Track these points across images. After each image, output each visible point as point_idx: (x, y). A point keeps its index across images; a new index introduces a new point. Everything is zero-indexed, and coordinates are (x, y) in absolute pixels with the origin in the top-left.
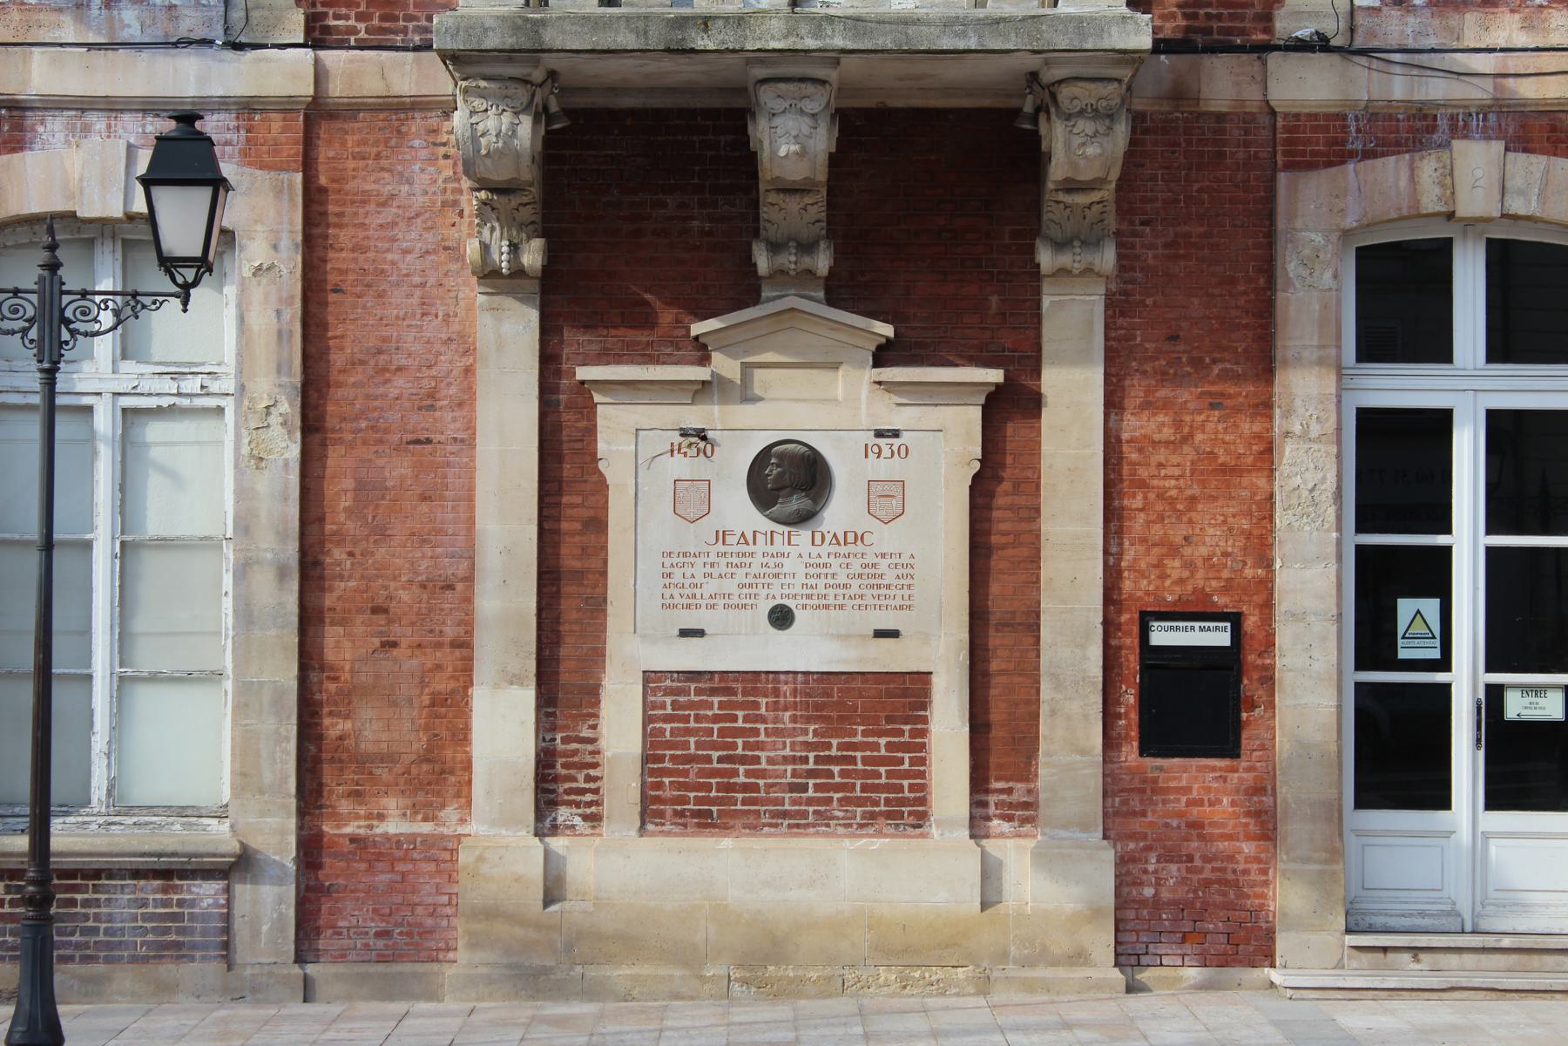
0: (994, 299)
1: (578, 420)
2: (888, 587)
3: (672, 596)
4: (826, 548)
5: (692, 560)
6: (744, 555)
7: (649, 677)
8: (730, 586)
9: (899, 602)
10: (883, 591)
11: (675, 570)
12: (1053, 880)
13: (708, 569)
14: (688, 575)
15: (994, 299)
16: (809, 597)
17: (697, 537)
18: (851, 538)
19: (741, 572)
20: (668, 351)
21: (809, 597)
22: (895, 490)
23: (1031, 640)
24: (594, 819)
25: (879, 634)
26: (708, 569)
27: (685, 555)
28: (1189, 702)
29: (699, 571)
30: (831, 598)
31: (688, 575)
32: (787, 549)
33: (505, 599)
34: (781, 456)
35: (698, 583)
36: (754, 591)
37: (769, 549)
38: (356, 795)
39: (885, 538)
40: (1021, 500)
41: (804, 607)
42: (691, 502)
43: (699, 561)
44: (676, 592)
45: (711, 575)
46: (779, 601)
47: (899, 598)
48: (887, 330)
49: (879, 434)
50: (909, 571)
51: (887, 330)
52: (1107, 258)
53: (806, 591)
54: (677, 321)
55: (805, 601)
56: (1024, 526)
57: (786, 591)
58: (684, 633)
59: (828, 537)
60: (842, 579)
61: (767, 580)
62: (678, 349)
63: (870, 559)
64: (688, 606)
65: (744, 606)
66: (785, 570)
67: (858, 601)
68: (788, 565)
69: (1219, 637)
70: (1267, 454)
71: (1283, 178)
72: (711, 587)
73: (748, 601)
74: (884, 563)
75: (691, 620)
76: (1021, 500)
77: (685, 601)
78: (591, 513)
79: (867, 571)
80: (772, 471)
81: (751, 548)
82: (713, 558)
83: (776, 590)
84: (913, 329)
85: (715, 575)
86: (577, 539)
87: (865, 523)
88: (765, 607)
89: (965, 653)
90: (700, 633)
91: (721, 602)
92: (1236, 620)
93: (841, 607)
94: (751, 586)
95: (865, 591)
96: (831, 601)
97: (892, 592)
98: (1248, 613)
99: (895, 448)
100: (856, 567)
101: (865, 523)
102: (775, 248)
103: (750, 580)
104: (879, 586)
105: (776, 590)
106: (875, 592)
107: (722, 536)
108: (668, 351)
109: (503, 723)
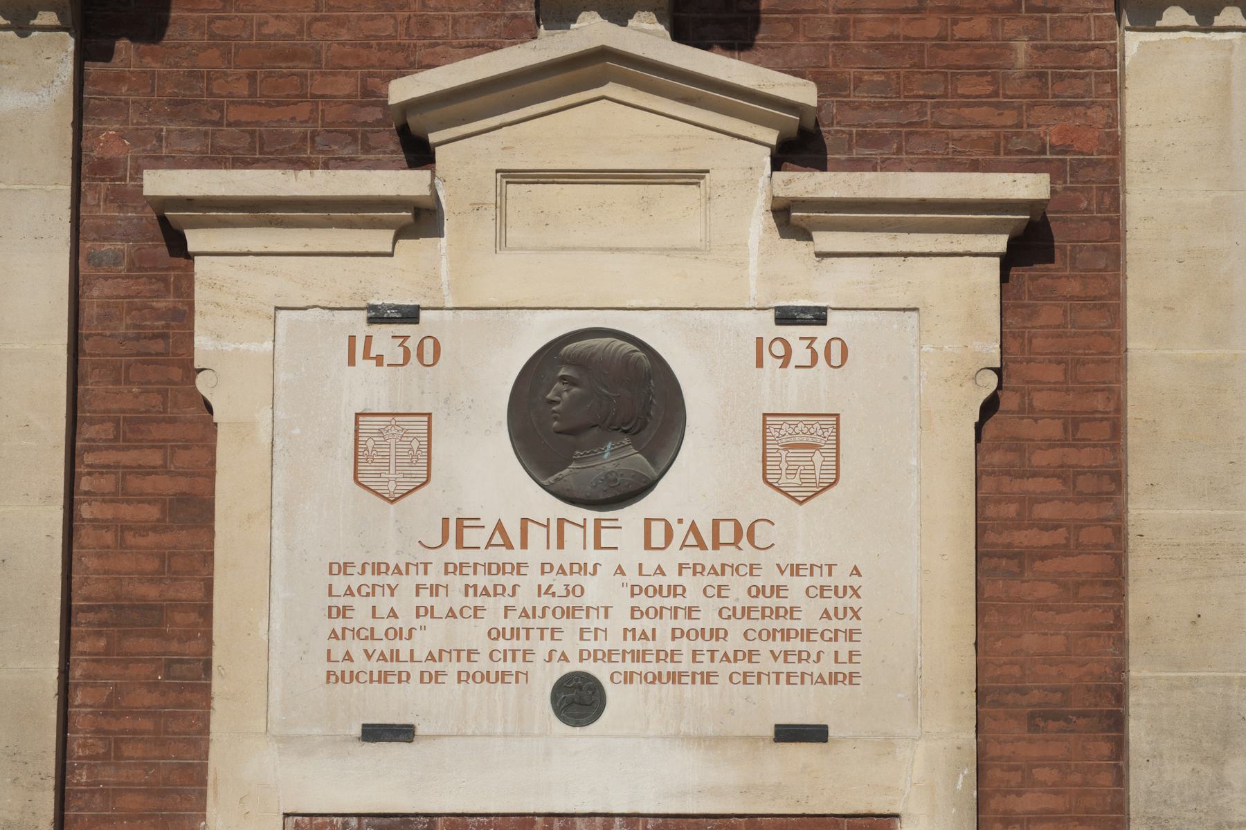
0: (1022, 48)
1: (157, 295)
2: (806, 635)
3: (348, 657)
4: (673, 556)
5: (391, 579)
6: (501, 569)
8: (471, 634)
9: (827, 666)
10: (796, 644)
11: (356, 601)
13: (426, 599)
14: (383, 610)
15: (1022, 48)
16: (639, 656)
17: (400, 531)
18: (727, 533)
20: (346, 153)
21: (639, 656)
22: (819, 432)
23: (1106, 748)
25: (787, 734)
26: (426, 599)
27: (377, 569)
29: (406, 602)
30: (686, 658)
31: (383, 610)
32: (592, 556)
34: (581, 362)
36: (521, 644)
39: (799, 533)
40: (1083, 458)
41: (629, 678)
43: (407, 583)
44: (356, 647)
45: (430, 612)
46: (574, 666)
47: (828, 659)
49: (786, 317)
53: (630, 645)
54: (366, 92)
55: (629, 666)
56: (1090, 510)
57: (591, 646)
58: (373, 733)
59: (680, 532)
60: (708, 619)
61: (550, 622)
62: (367, 149)
63: (770, 577)
64: (383, 677)
65: (502, 677)
66: (586, 601)
67: (743, 666)
68: (595, 590)
72: (431, 636)
73: (510, 666)
74: (796, 586)
75: (387, 707)
76: (1083, 458)
77: (376, 666)
78: (183, 484)
79: (761, 602)
80: (561, 394)
81: (516, 555)
83: (569, 642)
84: (855, 107)
85: (441, 610)
86: (152, 538)
88: (546, 677)
89: (970, 771)
90: (403, 733)
93: (707, 678)
94: (515, 633)
95: (757, 645)
96: (685, 664)
97: (813, 648)
99: (819, 347)
100: (738, 594)
101: (758, 502)
103: (514, 621)
104: (786, 635)
105: (569, 642)
106: (778, 646)
107: (455, 529)
108: (346, 153)
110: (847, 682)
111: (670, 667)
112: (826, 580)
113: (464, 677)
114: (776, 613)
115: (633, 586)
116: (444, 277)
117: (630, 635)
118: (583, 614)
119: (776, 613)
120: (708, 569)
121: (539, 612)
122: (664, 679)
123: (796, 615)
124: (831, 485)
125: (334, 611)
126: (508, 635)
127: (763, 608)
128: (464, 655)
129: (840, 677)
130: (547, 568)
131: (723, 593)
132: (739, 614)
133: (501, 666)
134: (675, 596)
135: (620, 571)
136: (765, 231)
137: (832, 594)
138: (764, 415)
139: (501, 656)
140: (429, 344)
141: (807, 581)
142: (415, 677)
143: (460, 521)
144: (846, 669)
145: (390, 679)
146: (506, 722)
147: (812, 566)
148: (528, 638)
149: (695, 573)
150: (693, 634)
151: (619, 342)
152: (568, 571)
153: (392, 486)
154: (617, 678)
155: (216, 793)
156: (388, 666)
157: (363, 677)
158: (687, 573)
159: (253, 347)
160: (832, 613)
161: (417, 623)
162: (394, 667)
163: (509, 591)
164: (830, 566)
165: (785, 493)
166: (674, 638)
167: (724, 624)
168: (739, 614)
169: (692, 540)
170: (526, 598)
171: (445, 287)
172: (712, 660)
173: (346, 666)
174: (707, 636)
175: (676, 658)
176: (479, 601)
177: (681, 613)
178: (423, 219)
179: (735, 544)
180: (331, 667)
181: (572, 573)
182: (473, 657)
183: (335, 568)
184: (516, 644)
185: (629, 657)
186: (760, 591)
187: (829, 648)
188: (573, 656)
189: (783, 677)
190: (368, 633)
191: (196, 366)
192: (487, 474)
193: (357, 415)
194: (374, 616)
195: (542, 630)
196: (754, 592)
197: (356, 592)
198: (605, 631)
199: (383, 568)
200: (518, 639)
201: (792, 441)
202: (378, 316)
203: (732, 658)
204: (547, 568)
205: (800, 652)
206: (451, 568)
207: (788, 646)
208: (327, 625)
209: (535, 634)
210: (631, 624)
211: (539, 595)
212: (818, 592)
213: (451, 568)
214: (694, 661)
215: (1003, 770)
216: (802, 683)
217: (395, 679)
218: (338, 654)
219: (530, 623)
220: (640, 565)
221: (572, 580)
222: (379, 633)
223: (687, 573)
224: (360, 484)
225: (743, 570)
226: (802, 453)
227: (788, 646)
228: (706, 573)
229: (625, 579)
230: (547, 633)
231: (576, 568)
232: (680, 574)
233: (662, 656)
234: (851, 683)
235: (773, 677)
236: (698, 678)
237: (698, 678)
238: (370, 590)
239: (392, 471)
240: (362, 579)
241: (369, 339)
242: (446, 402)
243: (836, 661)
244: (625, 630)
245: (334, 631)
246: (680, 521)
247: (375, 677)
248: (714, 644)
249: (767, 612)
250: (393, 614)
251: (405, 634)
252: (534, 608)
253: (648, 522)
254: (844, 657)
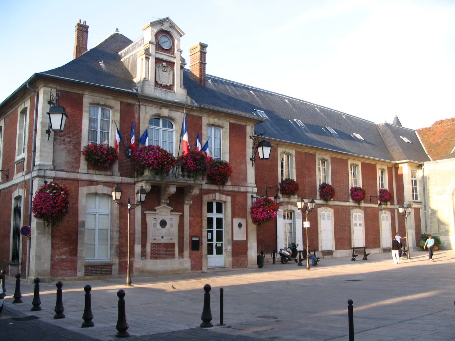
7: (151, 244)
12: (186, 263)
24: (146, 258)
28: (196, 246)
33: (138, 235)
35: (156, 234)
38: (124, 256)
39: (171, 229)
42: (155, 225)
48: (172, 209)
51: (172, 209)
52: (191, 202)
68: (163, 232)
69: (198, 239)
70: (202, 221)
71: (203, 196)
75: (155, 238)
92: (199, 237)
98: (200, 236)
101: (170, 228)
102: (164, 200)
109: (138, 248)
178: (156, 214)
192: (159, 226)
226: (171, 225)
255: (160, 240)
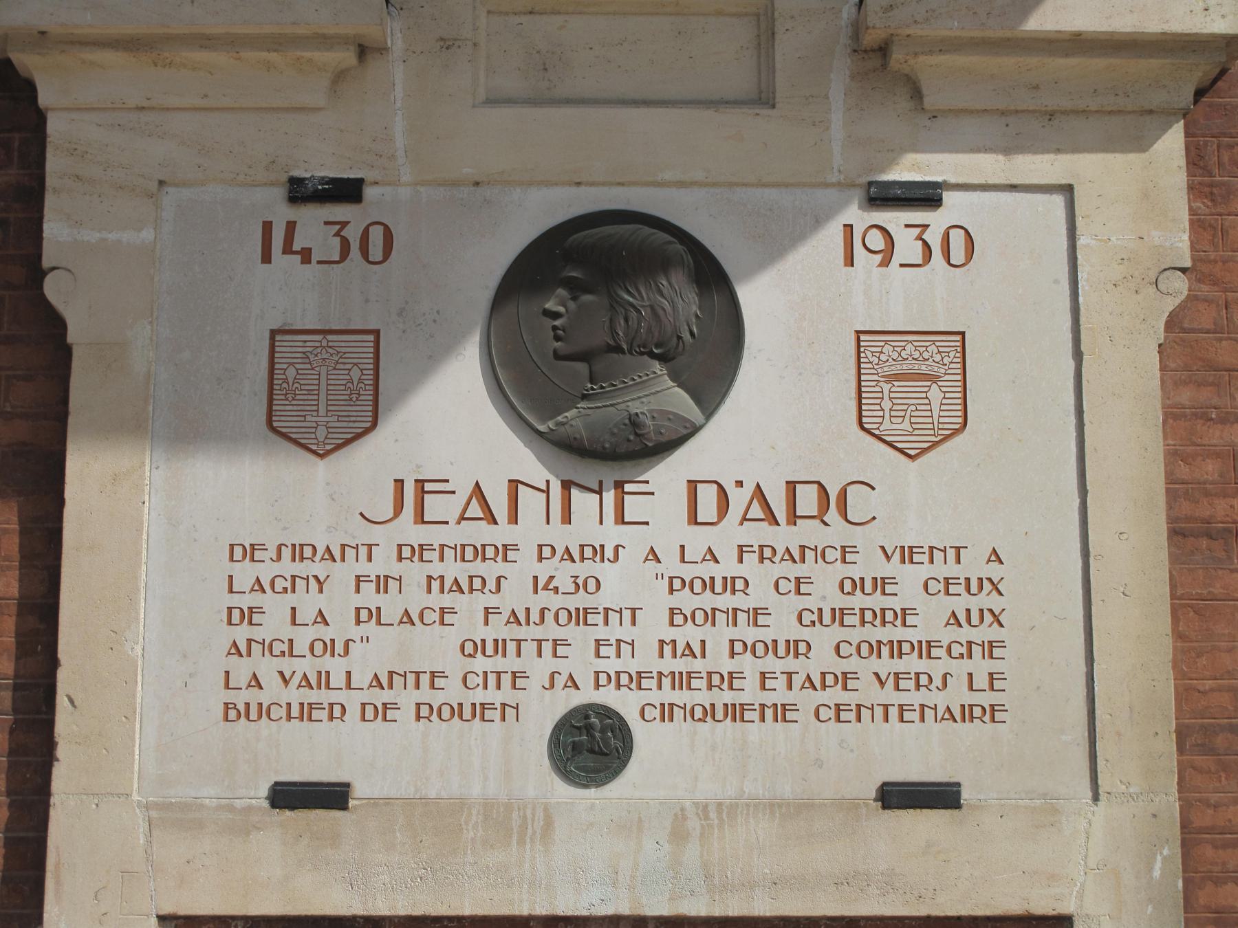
2: (925, 649)
3: (255, 682)
4: (728, 535)
6: (480, 553)
8: (436, 648)
9: (958, 695)
10: (912, 663)
11: (267, 600)
13: (369, 597)
14: (307, 614)
16: (682, 681)
18: (807, 500)
19: (469, 606)
21: (682, 681)
22: (936, 356)
26: (369, 597)
27: (298, 553)
29: (340, 600)
30: (750, 683)
32: (611, 534)
36: (509, 663)
37: (559, 535)
39: (911, 501)
41: (667, 712)
44: (267, 668)
45: (376, 615)
46: (587, 695)
47: (958, 686)
50: (987, 600)
53: (670, 664)
55: (669, 695)
57: (612, 665)
59: (739, 499)
60: (782, 626)
61: (551, 630)
63: (868, 566)
64: (307, 712)
66: (603, 599)
67: (835, 695)
68: (617, 584)
72: (376, 652)
73: (493, 696)
74: (909, 579)
75: (309, 756)
77: (295, 695)
79: (858, 601)
81: (501, 533)
82: (384, 563)
83: (578, 660)
85: (392, 613)
87: (850, 457)
88: (544, 711)
91: (407, 698)
93: (782, 712)
94: (500, 647)
96: (749, 693)
97: (937, 669)
101: (850, 457)
103: (498, 629)
104: (896, 649)
105: (579, 660)
106: (886, 665)
107: (414, 495)
110: (987, 718)
111: (728, 697)
112: (952, 570)
113: (425, 711)
114: (881, 617)
115: (671, 578)
116: (400, 142)
117: (668, 649)
118: (600, 619)
119: (881, 617)
120: (780, 551)
121: (535, 617)
122: (720, 715)
123: (910, 620)
124: (956, 432)
125: (236, 614)
126: (490, 650)
127: (862, 610)
128: (425, 679)
129: (977, 712)
130: (547, 552)
131: (803, 588)
132: (827, 619)
133: (479, 696)
134: (734, 591)
135: (653, 555)
136: (852, 78)
137: (961, 589)
138: (858, 332)
139: (480, 680)
140: (376, 235)
141: (925, 571)
142: (354, 711)
143: (420, 483)
144: (986, 699)
145: (316, 714)
146: (486, 779)
147: (931, 548)
148: (519, 655)
149: (762, 559)
150: (760, 648)
151: (647, 230)
152: (577, 557)
153: (321, 433)
154: (651, 713)
155: (58, 882)
156: (313, 696)
157: (276, 712)
158: (751, 559)
159: (127, 236)
160: (962, 618)
161: (355, 632)
162: (323, 697)
163: (491, 585)
164: (958, 549)
165: (890, 444)
166: (732, 654)
167: (806, 633)
168: (827, 619)
169: (756, 511)
170: (516, 596)
171: (400, 153)
172: (790, 687)
173: (253, 696)
174: (781, 650)
175: (736, 683)
176: (447, 600)
177: (742, 617)
179: (820, 517)
180: (230, 696)
181: (583, 559)
182: (439, 682)
183: (238, 552)
184: (499, 663)
185: (666, 682)
186: (858, 585)
187: (960, 669)
188: (585, 681)
189: (894, 712)
190: (285, 647)
191: (46, 263)
193: (273, 333)
194: (294, 623)
195: (540, 642)
196: (848, 586)
197: (267, 587)
198: (632, 644)
199: (308, 552)
200: (504, 655)
201: (898, 369)
202: (301, 192)
203: (818, 684)
204: (547, 552)
205: (917, 674)
206: (406, 552)
207: (899, 665)
208: (227, 635)
209: (529, 648)
210: (669, 634)
211: (536, 592)
212: (941, 587)
213: (406, 552)
214: (763, 688)
215: (1216, 847)
216: (923, 719)
217: (324, 715)
218: (241, 676)
219: (522, 632)
220: (682, 547)
221: (583, 570)
222: (301, 647)
223: (751, 559)
224: (275, 430)
225: (831, 555)
227: (899, 665)
228: (777, 559)
229: (660, 568)
230: (547, 648)
231: (588, 552)
232: (741, 561)
233: (716, 680)
234: (993, 720)
235: (879, 711)
236: (769, 713)
237: (769, 713)
238: (288, 585)
239: (322, 411)
240: (276, 569)
241: (291, 227)
242: (400, 314)
243: (971, 688)
244: (662, 642)
245: (235, 644)
246: (740, 484)
247: (295, 712)
248: (791, 664)
249: (868, 616)
250: (322, 618)
251: (339, 648)
252: (528, 609)
253: (693, 485)
254: (981, 681)
255: (507, 822)
